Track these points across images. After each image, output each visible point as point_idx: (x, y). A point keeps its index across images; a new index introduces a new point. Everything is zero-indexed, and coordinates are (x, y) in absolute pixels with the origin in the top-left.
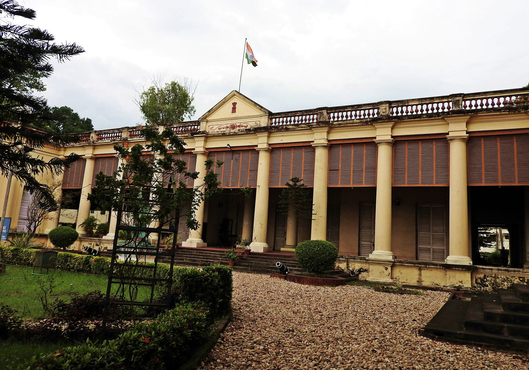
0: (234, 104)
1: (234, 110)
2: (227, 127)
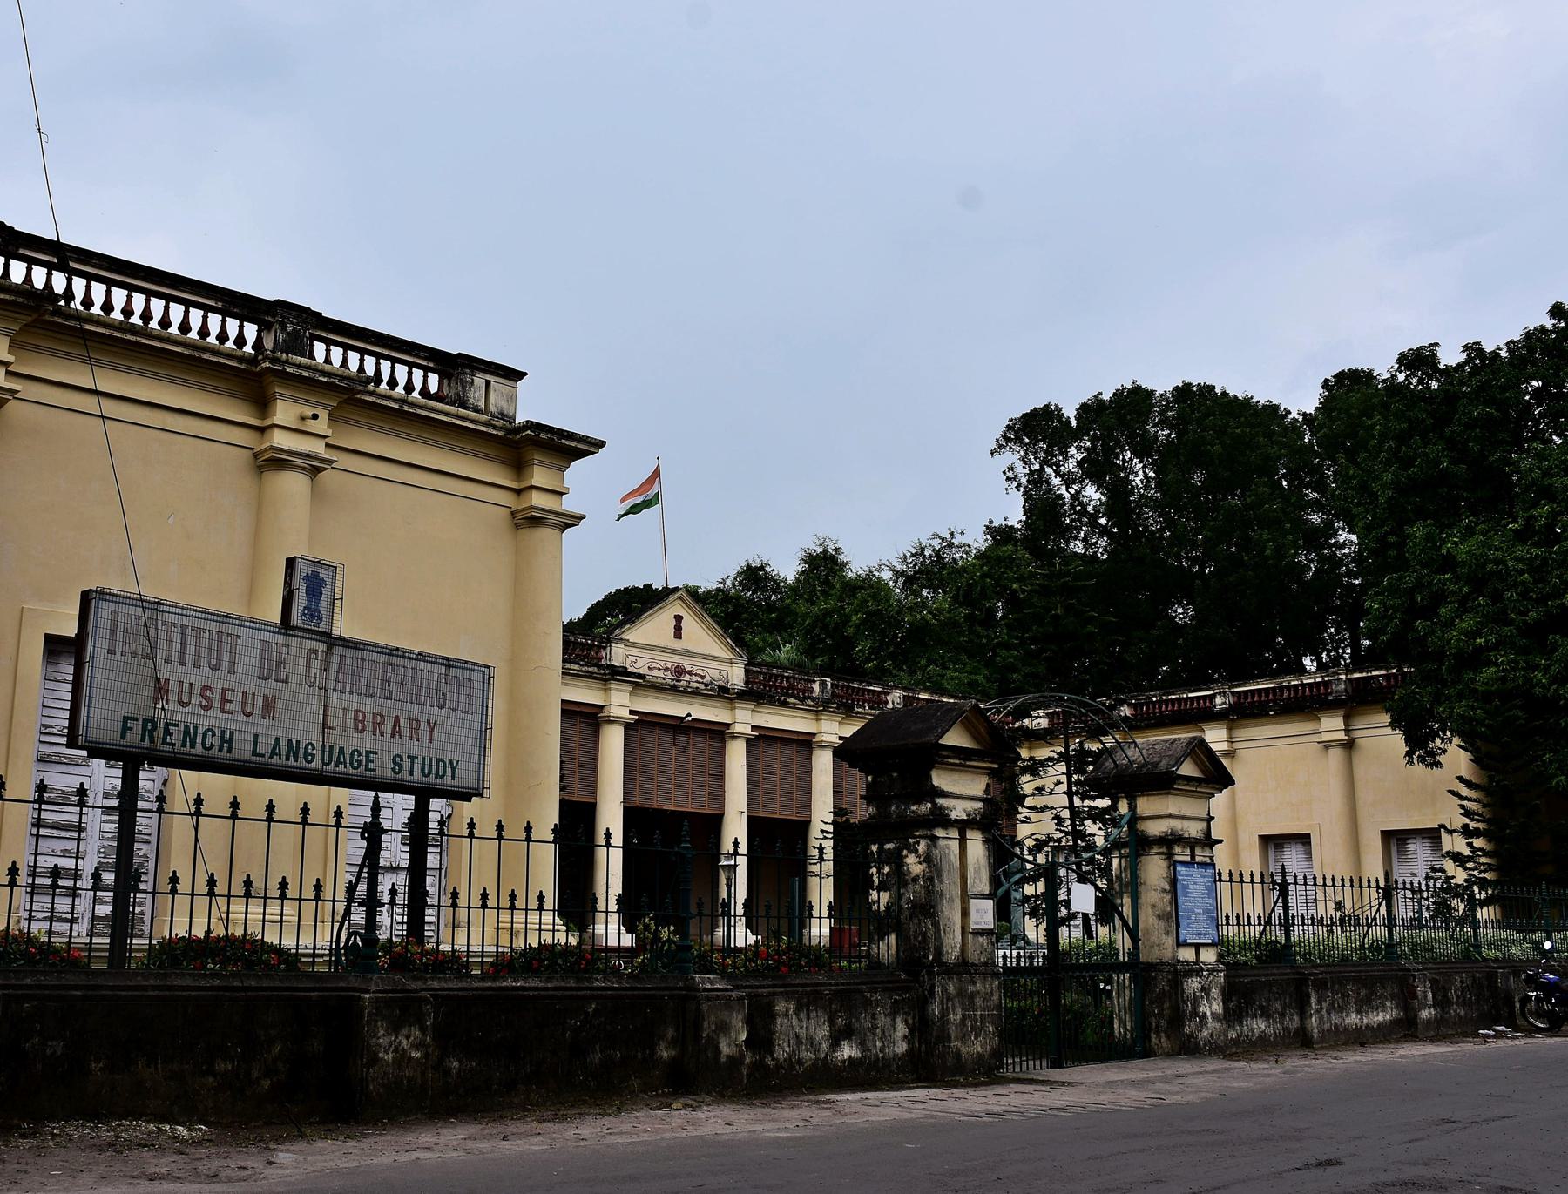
0: (679, 619)
1: (678, 633)
2: (667, 669)
